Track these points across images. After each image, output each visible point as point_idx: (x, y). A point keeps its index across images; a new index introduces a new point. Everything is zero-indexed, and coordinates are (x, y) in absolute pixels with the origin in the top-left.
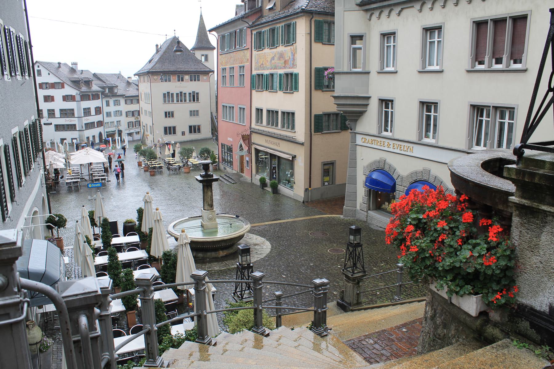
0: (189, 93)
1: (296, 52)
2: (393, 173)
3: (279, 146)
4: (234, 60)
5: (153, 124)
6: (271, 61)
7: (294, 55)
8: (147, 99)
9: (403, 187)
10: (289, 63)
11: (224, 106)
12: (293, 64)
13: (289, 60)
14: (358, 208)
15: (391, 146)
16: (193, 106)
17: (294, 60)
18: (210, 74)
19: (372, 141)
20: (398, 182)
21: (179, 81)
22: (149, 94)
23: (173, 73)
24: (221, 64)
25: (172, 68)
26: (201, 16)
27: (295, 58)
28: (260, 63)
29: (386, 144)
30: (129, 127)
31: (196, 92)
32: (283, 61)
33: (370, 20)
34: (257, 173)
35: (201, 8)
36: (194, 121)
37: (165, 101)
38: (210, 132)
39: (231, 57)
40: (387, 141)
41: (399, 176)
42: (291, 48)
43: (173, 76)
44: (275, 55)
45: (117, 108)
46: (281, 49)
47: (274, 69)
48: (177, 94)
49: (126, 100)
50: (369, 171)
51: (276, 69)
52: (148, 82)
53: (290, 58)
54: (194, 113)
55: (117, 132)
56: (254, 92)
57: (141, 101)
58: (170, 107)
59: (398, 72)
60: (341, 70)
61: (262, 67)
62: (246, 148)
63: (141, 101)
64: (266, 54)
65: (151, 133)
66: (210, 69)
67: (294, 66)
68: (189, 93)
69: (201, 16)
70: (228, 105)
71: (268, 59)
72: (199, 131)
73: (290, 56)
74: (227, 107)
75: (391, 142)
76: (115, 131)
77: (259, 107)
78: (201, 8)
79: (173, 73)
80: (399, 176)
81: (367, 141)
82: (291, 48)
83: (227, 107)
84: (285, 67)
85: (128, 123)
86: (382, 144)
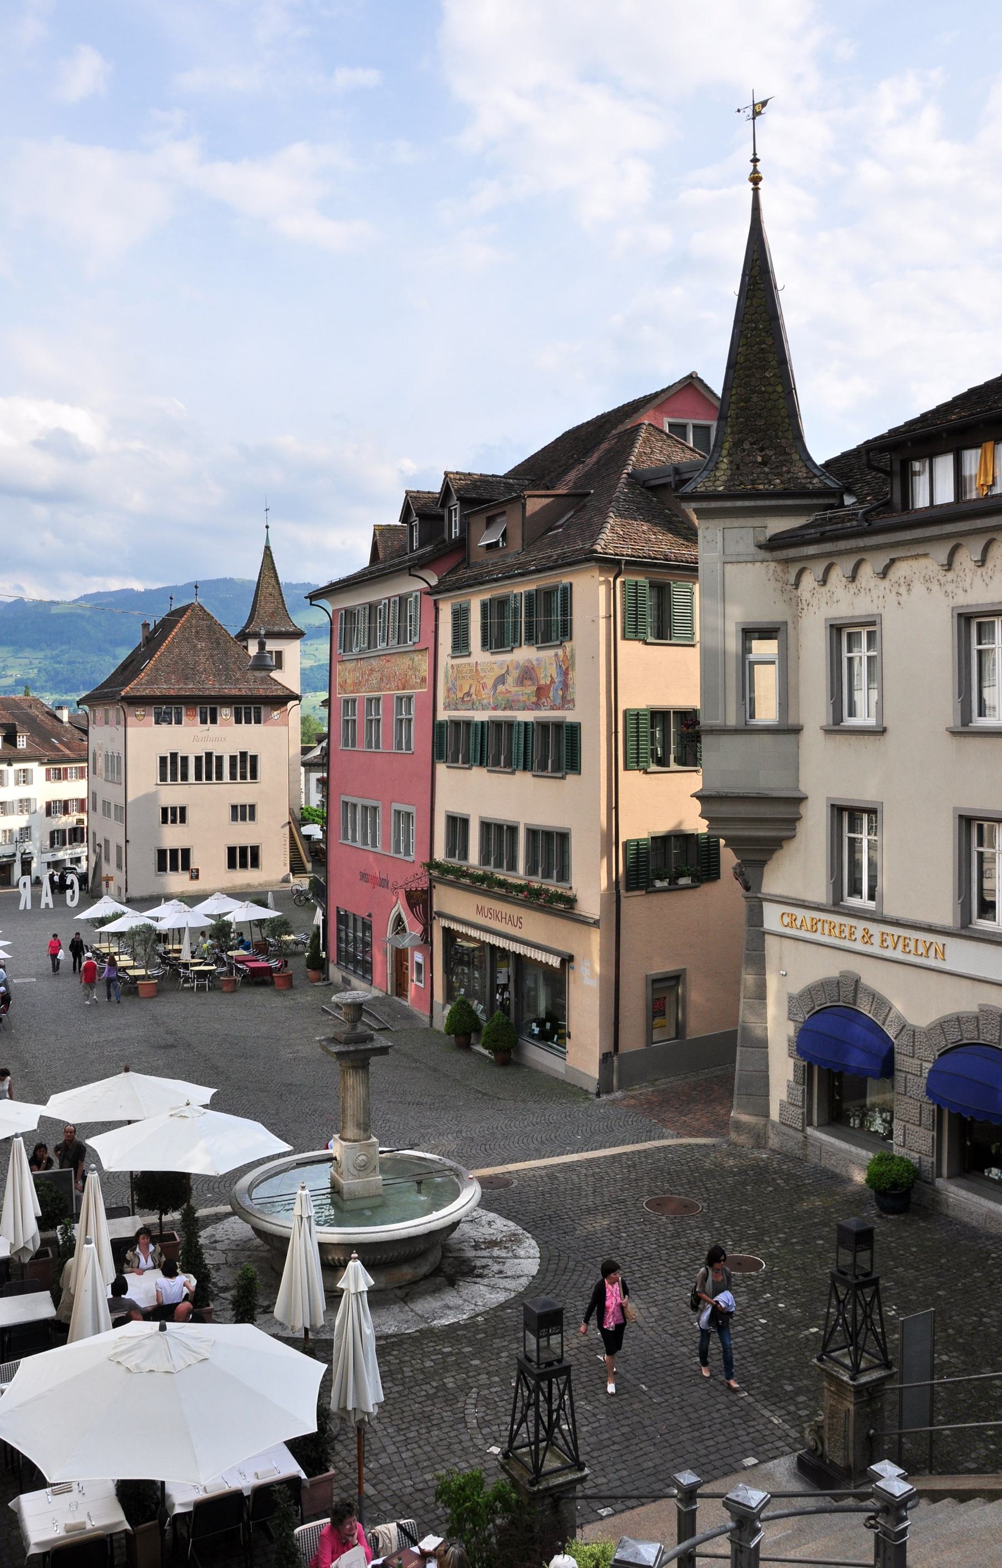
0: (231, 757)
1: (573, 664)
2: (885, 1021)
3: (519, 925)
4: (381, 679)
5: (127, 841)
6: (495, 687)
7: (566, 674)
8: (113, 772)
9: (919, 1062)
10: (551, 694)
11: (346, 803)
13: (549, 686)
14: (775, 1114)
15: (876, 940)
16: (242, 793)
17: (565, 686)
18: (291, 704)
19: (815, 922)
20: (901, 1045)
21: (204, 721)
22: (119, 757)
23: (191, 701)
24: (341, 686)
25: (189, 688)
26: (267, 548)
27: (570, 683)
28: (461, 691)
29: (859, 933)
30: (52, 845)
31: (249, 754)
32: (530, 689)
33: (797, 585)
34: (447, 999)
35: (267, 527)
36: (243, 835)
37: (163, 778)
38: (285, 865)
39: (372, 670)
40: (861, 925)
41: (904, 1027)
42: (556, 655)
43: (187, 709)
44: (507, 672)
45: (23, 792)
46: (525, 654)
47: (505, 709)
48: (198, 759)
49: (48, 771)
50: (808, 1009)
51: (511, 708)
52: (118, 723)
53: (552, 681)
54: (243, 813)
55: (18, 857)
56: (441, 768)
57: (95, 773)
58: (173, 795)
59: (890, 730)
60: (718, 722)
61: (467, 701)
62: (414, 930)
63: (95, 773)
64: (479, 668)
65: (119, 866)
66: (287, 689)
68: (231, 757)
69: (267, 548)
70: (360, 802)
71: (485, 680)
72: (255, 864)
73: (555, 676)
74: (355, 806)
75: (875, 929)
76: (14, 855)
77: (459, 809)
78: (267, 527)
79: (191, 701)
80: (904, 1027)
81: (798, 923)
82: (556, 655)
83: (355, 806)
84: (537, 706)
85: (52, 833)
86: (847, 933)
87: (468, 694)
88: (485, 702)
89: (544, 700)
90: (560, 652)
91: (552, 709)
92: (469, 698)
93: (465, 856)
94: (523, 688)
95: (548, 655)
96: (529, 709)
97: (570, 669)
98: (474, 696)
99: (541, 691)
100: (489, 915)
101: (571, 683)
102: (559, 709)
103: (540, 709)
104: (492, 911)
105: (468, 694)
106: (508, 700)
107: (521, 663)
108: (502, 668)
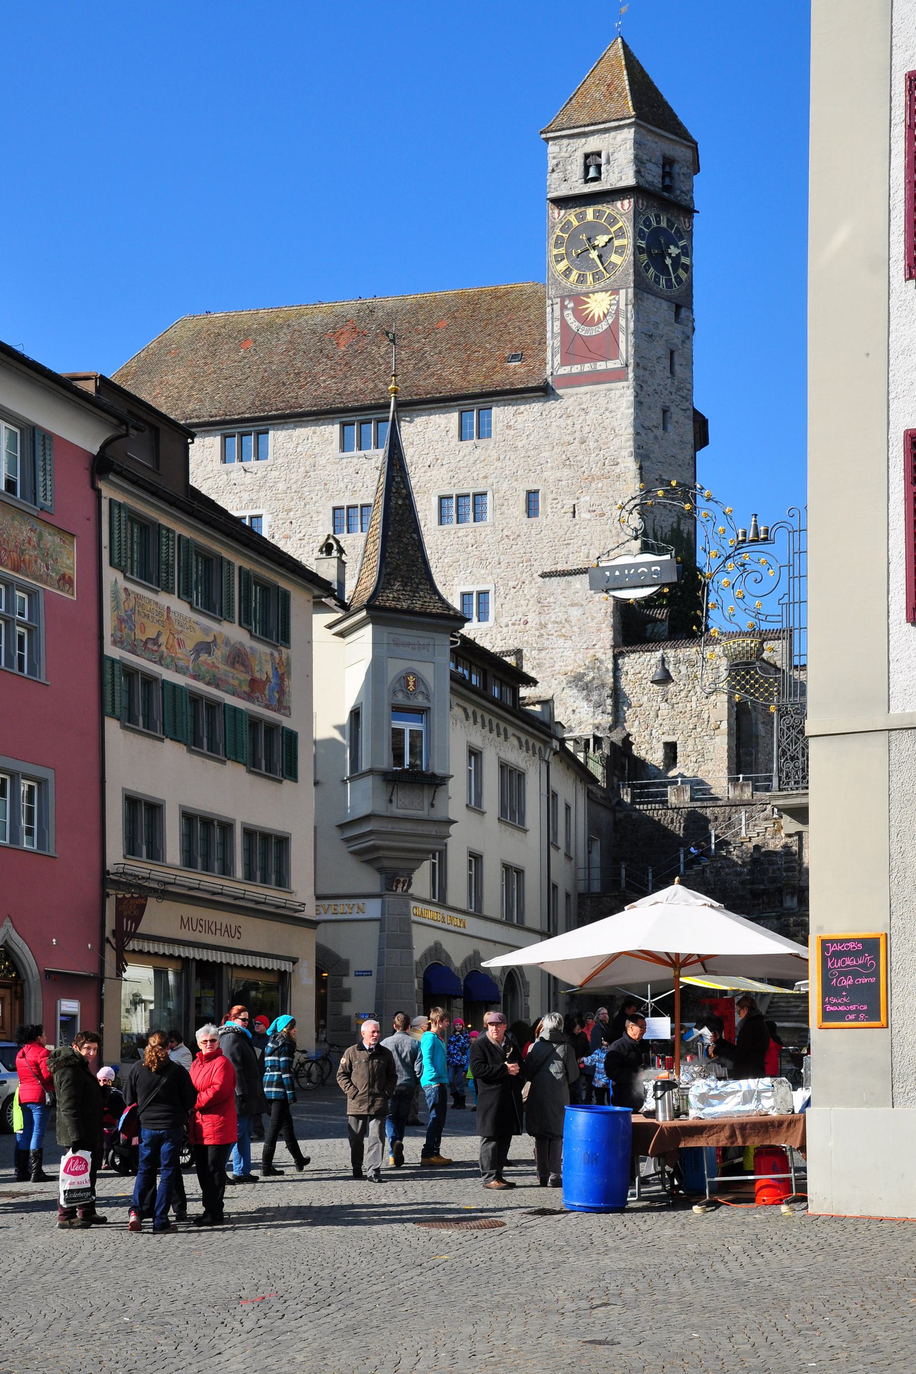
1: (289, 674)
3: (238, 935)
10: (267, 692)
12: (280, 701)
17: (282, 691)
42: (272, 655)
44: (215, 641)
47: (208, 684)
51: (217, 686)
64: (172, 615)
67: (282, 707)
73: (271, 676)
77: (145, 788)
84: (249, 697)
87: (155, 641)
88: (181, 663)
89: (257, 694)
90: (276, 654)
91: (267, 707)
92: (155, 648)
93: (155, 853)
94: (235, 672)
95: (263, 649)
96: (240, 697)
97: (286, 676)
98: (163, 648)
99: (253, 682)
100: (199, 928)
101: (287, 690)
102: (275, 711)
103: (253, 703)
104: (203, 923)
105: (155, 641)
106: (214, 676)
107: (232, 642)
108: (207, 635)
